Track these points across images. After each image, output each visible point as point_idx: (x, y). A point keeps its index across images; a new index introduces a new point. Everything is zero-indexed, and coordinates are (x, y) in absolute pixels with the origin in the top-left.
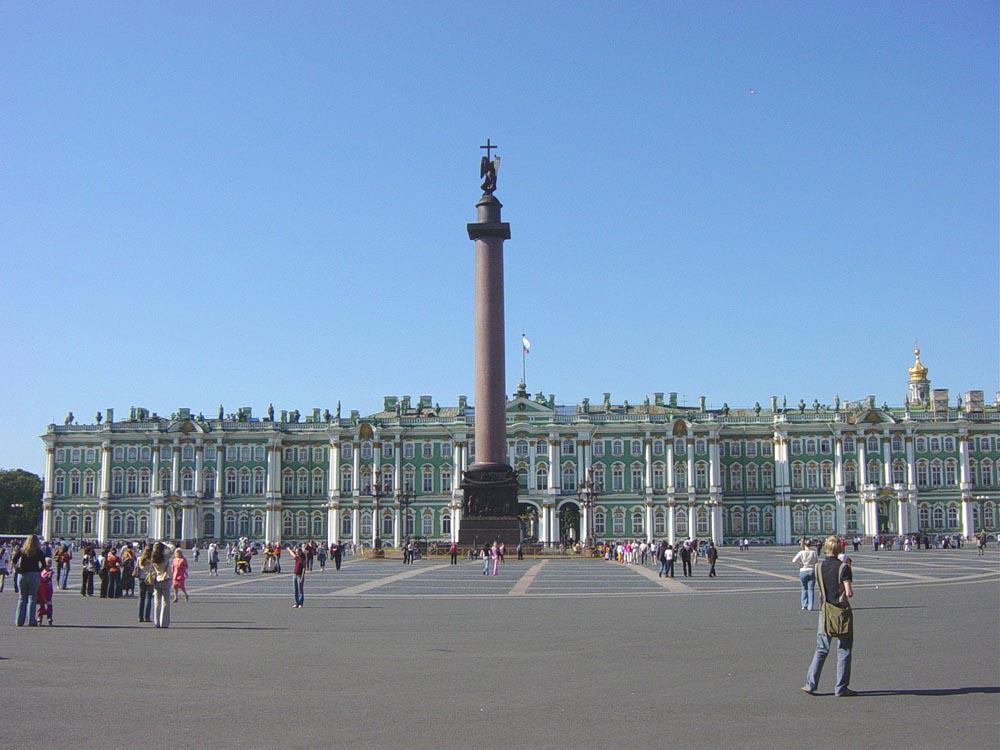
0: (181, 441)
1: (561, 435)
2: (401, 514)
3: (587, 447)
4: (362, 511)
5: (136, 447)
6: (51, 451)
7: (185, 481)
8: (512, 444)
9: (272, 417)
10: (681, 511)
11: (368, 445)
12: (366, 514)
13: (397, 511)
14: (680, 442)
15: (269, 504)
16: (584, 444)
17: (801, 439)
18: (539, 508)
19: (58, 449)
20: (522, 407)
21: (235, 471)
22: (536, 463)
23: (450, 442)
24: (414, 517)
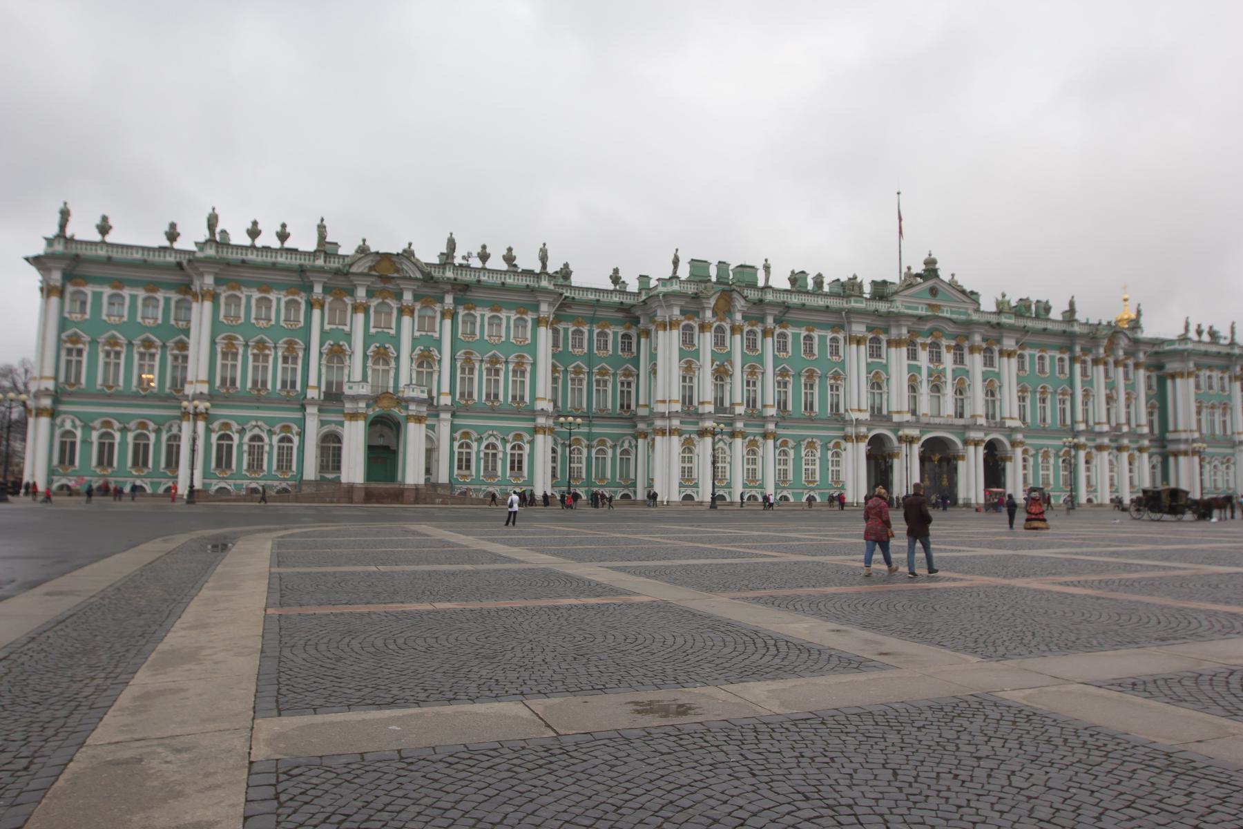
0: (371, 294)
2: (775, 447)
5: (273, 296)
6: (48, 291)
7: (374, 370)
8: (924, 345)
9: (544, 266)
11: (720, 329)
13: (770, 442)
14: (1106, 364)
18: (960, 445)
19: (70, 289)
20: (933, 292)
21: (477, 356)
23: (841, 336)
24: (792, 452)
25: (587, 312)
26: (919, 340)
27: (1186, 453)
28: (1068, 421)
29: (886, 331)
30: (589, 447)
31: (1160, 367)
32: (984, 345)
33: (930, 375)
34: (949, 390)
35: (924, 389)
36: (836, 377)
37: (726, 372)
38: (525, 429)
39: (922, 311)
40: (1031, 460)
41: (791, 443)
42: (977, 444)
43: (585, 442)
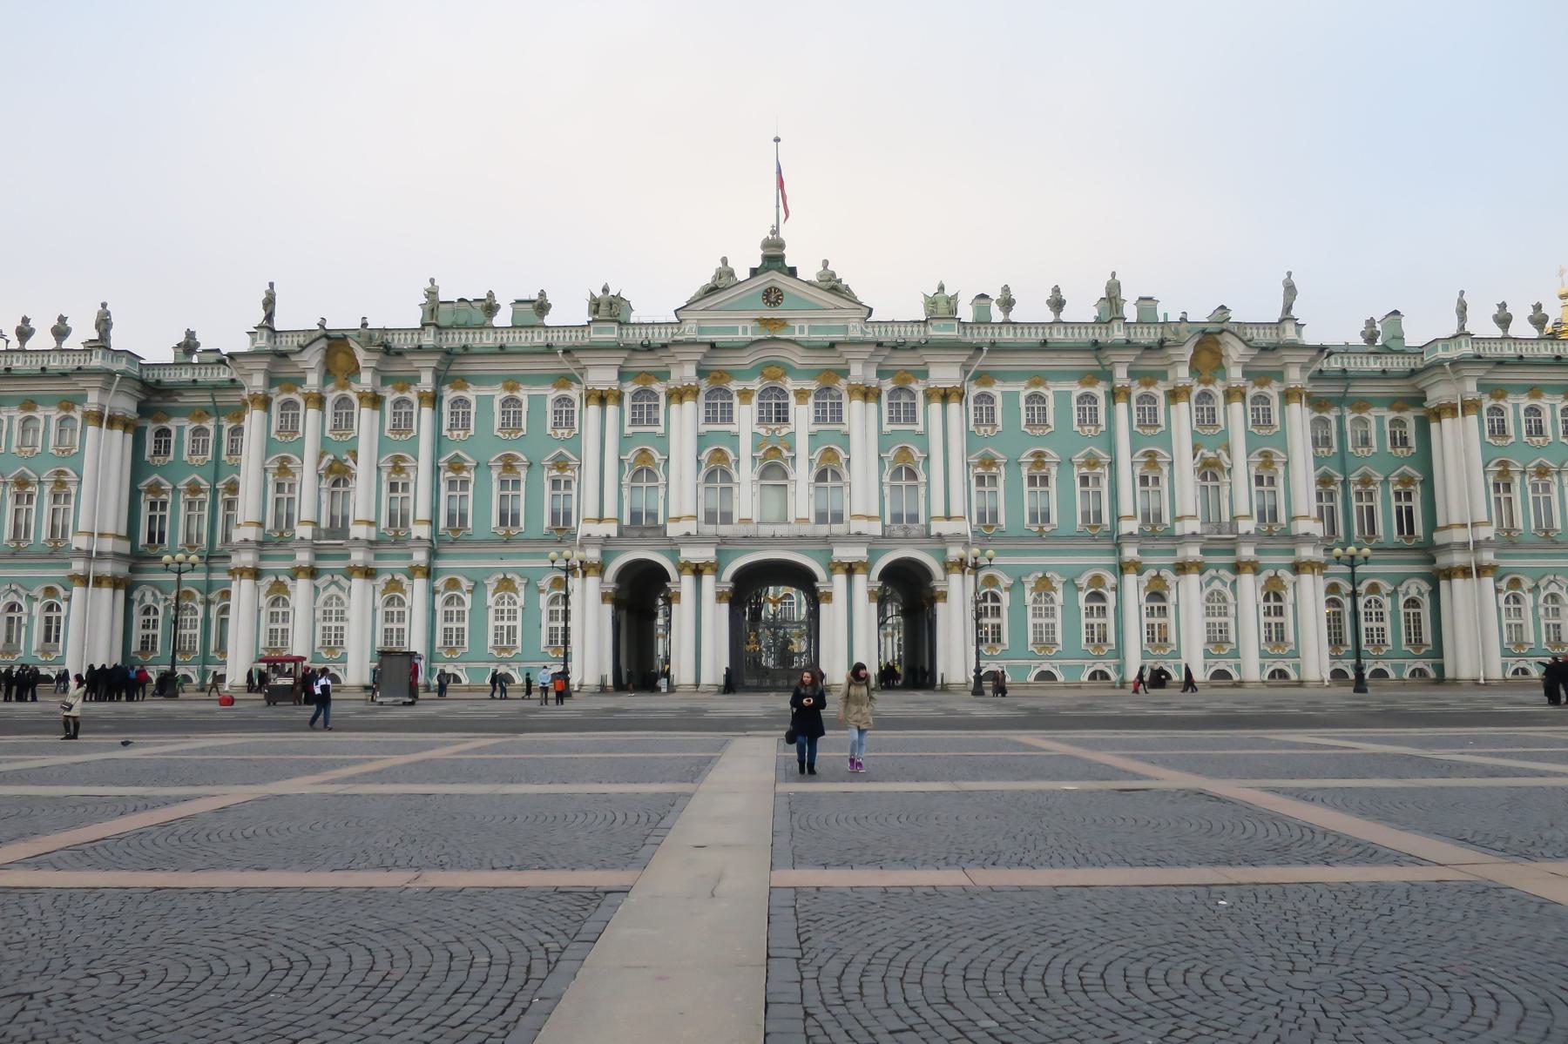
1: (881, 374)
2: (433, 592)
3: (954, 407)
4: (322, 581)
8: (745, 395)
10: (1216, 585)
11: (343, 402)
12: (333, 590)
14: (1205, 396)
15: (78, 566)
16: (945, 397)
17: (1508, 404)
20: (772, 296)
22: (811, 452)
23: (574, 393)
24: (468, 599)
25: (203, 399)
26: (734, 386)
27: (1466, 572)
28: (1106, 519)
29: (664, 376)
30: (208, 603)
31: (1418, 400)
32: (888, 385)
33: (756, 448)
34: (802, 474)
35: (746, 474)
36: (561, 464)
37: (347, 470)
38: (58, 580)
39: (746, 331)
40: (1005, 598)
41: (465, 584)
42: (850, 570)
43: (198, 597)
